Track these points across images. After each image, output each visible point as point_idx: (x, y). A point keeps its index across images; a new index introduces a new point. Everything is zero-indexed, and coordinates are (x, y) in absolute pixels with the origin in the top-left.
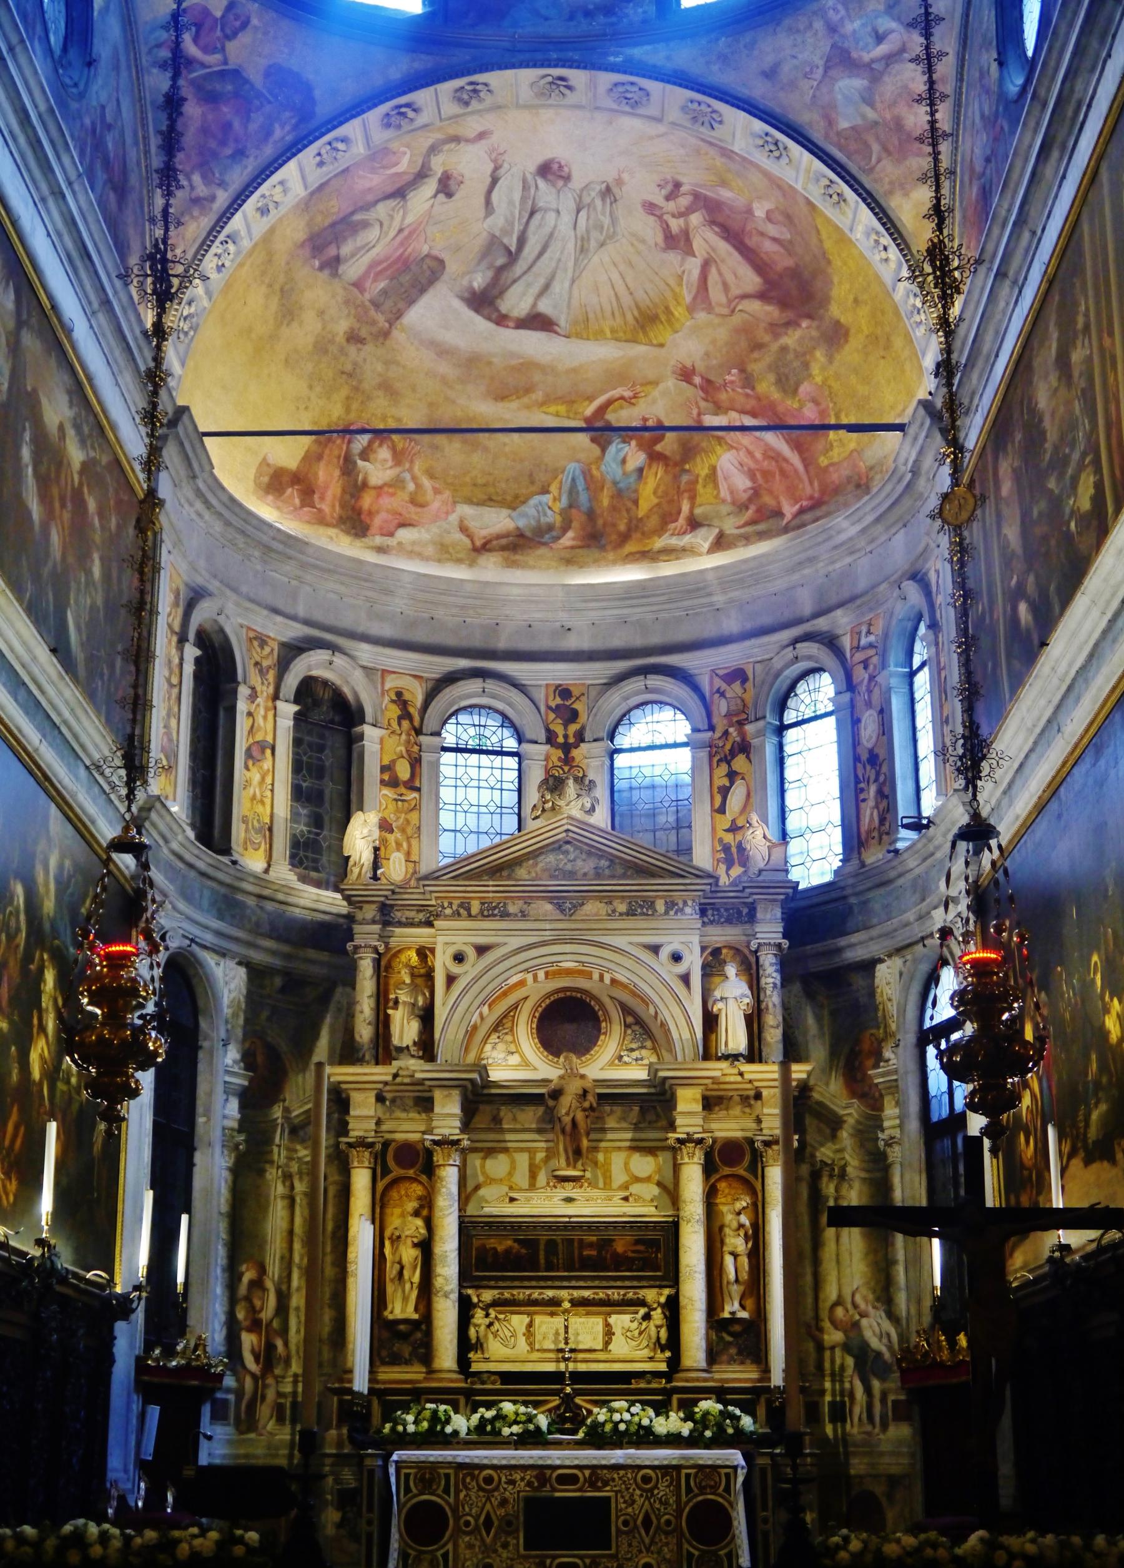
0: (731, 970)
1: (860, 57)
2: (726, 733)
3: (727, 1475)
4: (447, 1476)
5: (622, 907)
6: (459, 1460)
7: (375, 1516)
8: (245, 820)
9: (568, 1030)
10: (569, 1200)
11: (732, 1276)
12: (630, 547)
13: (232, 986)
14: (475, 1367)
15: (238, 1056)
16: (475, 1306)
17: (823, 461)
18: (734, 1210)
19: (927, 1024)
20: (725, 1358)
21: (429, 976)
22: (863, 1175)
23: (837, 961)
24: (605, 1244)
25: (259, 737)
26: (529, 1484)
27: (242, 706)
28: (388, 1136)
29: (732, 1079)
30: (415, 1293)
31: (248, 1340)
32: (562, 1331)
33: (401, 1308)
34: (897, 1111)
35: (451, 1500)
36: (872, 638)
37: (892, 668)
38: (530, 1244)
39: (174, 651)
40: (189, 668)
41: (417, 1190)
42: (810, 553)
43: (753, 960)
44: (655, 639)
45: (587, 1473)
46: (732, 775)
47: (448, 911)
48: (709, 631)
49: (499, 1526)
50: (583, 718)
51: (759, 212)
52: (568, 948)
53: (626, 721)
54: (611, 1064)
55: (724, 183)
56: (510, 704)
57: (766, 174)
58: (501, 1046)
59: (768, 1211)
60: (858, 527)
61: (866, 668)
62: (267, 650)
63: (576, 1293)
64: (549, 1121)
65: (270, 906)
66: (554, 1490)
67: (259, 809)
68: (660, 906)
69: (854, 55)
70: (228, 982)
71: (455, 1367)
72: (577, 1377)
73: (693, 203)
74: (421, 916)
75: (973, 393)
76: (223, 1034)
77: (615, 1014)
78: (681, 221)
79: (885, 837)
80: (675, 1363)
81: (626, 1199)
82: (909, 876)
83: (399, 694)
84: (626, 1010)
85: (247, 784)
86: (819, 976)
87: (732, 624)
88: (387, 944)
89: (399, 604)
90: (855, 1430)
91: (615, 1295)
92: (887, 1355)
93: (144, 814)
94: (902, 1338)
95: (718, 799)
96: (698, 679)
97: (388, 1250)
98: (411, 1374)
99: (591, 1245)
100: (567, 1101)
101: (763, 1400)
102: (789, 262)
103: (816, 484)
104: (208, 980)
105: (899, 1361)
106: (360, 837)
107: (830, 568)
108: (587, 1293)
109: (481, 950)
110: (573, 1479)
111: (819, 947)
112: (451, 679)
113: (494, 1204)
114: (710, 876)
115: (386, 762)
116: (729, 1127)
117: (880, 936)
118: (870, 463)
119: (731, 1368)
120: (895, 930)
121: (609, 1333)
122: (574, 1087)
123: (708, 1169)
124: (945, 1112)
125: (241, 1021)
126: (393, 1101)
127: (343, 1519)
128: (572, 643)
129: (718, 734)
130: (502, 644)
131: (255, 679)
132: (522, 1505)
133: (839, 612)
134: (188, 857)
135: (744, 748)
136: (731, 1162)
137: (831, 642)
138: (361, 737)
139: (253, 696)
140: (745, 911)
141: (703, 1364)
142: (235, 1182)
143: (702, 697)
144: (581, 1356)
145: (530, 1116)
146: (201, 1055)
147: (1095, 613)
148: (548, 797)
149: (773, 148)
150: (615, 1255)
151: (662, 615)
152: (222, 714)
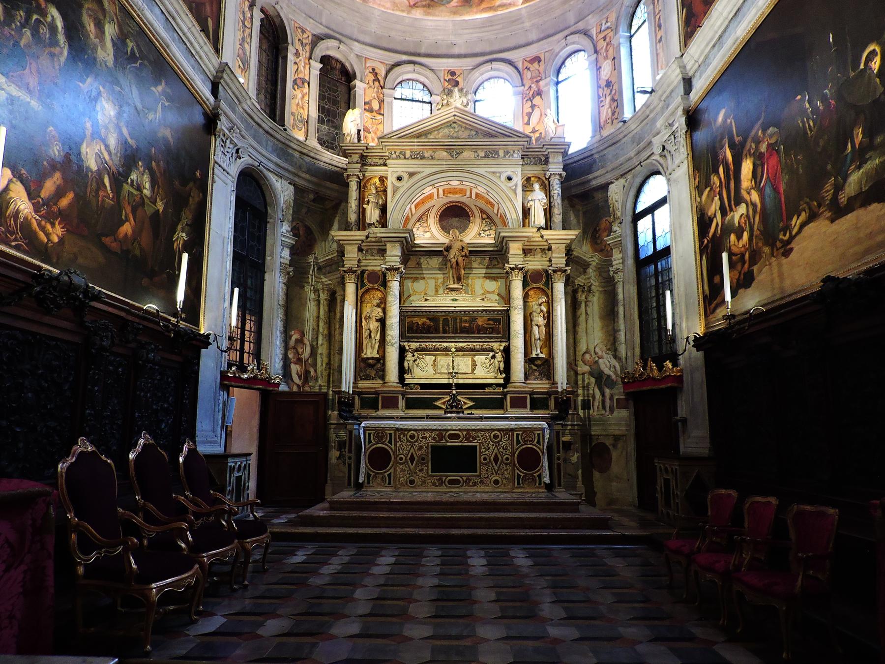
0: (537, 186)
2: (530, 87)
3: (539, 435)
4: (390, 434)
5: (482, 154)
6: (397, 426)
7: (353, 455)
8: (293, 114)
9: (455, 221)
10: (455, 300)
11: (537, 336)
12: (483, 6)
13: (286, 194)
14: (407, 381)
15: (289, 229)
16: (407, 351)
18: (537, 302)
20: (533, 377)
21: (385, 191)
22: (601, 289)
23: (587, 187)
24: (474, 320)
25: (301, 76)
26: (434, 439)
27: (291, 57)
28: (363, 268)
29: (537, 239)
30: (377, 345)
31: (295, 368)
32: (451, 364)
33: (371, 352)
34: (621, 256)
35: (393, 447)
36: (609, 24)
37: (621, 33)
38: (435, 320)
39: (247, 9)
40: (257, 23)
41: (379, 294)
43: (547, 183)
44: (496, 47)
45: (464, 433)
46: (533, 107)
47: (394, 156)
48: (522, 41)
49: (418, 461)
50: (461, 85)
52: (455, 174)
53: (481, 87)
54: (475, 237)
56: (427, 78)
58: (421, 229)
59: (555, 305)
62: (305, 35)
63: (458, 345)
64: (445, 264)
65: (307, 159)
66: (447, 442)
67: (301, 111)
68: (501, 153)
70: (283, 192)
71: (397, 380)
72: (459, 386)
74: (381, 161)
76: (280, 216)
77: (477, 213)
79: (615, 121)
80: (507, 380)
81: (483, 299)
82: (630, 135)
83: (373, 70)
84: (482, 212)
85: (294, 97)
86: (577, 196)
87: (533, 36)
88: (364, 175)
89: (373, 27)
90: (595, 413)
91: (478, 346)
92: (614, 377)
93: (220, 74)
94: (622, 367)
95: (526, 119)
96: (516, 64)
97: (364, 324)
98: (376, 384)
99: (466, 321)
100: (453, 253)
101: (552, 397)
104: (271, 187)
105: (623, 379)
106: (352, 121)
108: (463, 345)
109: (411, 175)
110: (458, 436)
111: (578, 181)
112: (398, 64)
113: (417, 302)
114: (528, 137)
115: (367, 100)
116: (535, 264)
117: (612, 170)
119: (535, 382)
120: (622, 164)
121: (474, 365)
122: (457, 246)
123: (525, 284)
124: (650, 251)
125: (291, 212)
126: (367, 251)
127: (340, 454)
128: (456, 51)
129: (527, 87)
130: (423, 50)
131: (298, 46)
132: (430, 450)
133: (590, 16)
134: (256, 118)
135: (539, 93)
136: (536, 282)
137: (586, 33)
138: (355, 87)
139: (297, 54)
140: (543, 159)
141: (523, 380)
142: (287, 290)
143: (519, 72)
144: (460, 376)
145: (435, 262)
146: (268, 225)
148: (445, 97)
150: (478, 326)
151: (499, 36)
152: (280, 60)
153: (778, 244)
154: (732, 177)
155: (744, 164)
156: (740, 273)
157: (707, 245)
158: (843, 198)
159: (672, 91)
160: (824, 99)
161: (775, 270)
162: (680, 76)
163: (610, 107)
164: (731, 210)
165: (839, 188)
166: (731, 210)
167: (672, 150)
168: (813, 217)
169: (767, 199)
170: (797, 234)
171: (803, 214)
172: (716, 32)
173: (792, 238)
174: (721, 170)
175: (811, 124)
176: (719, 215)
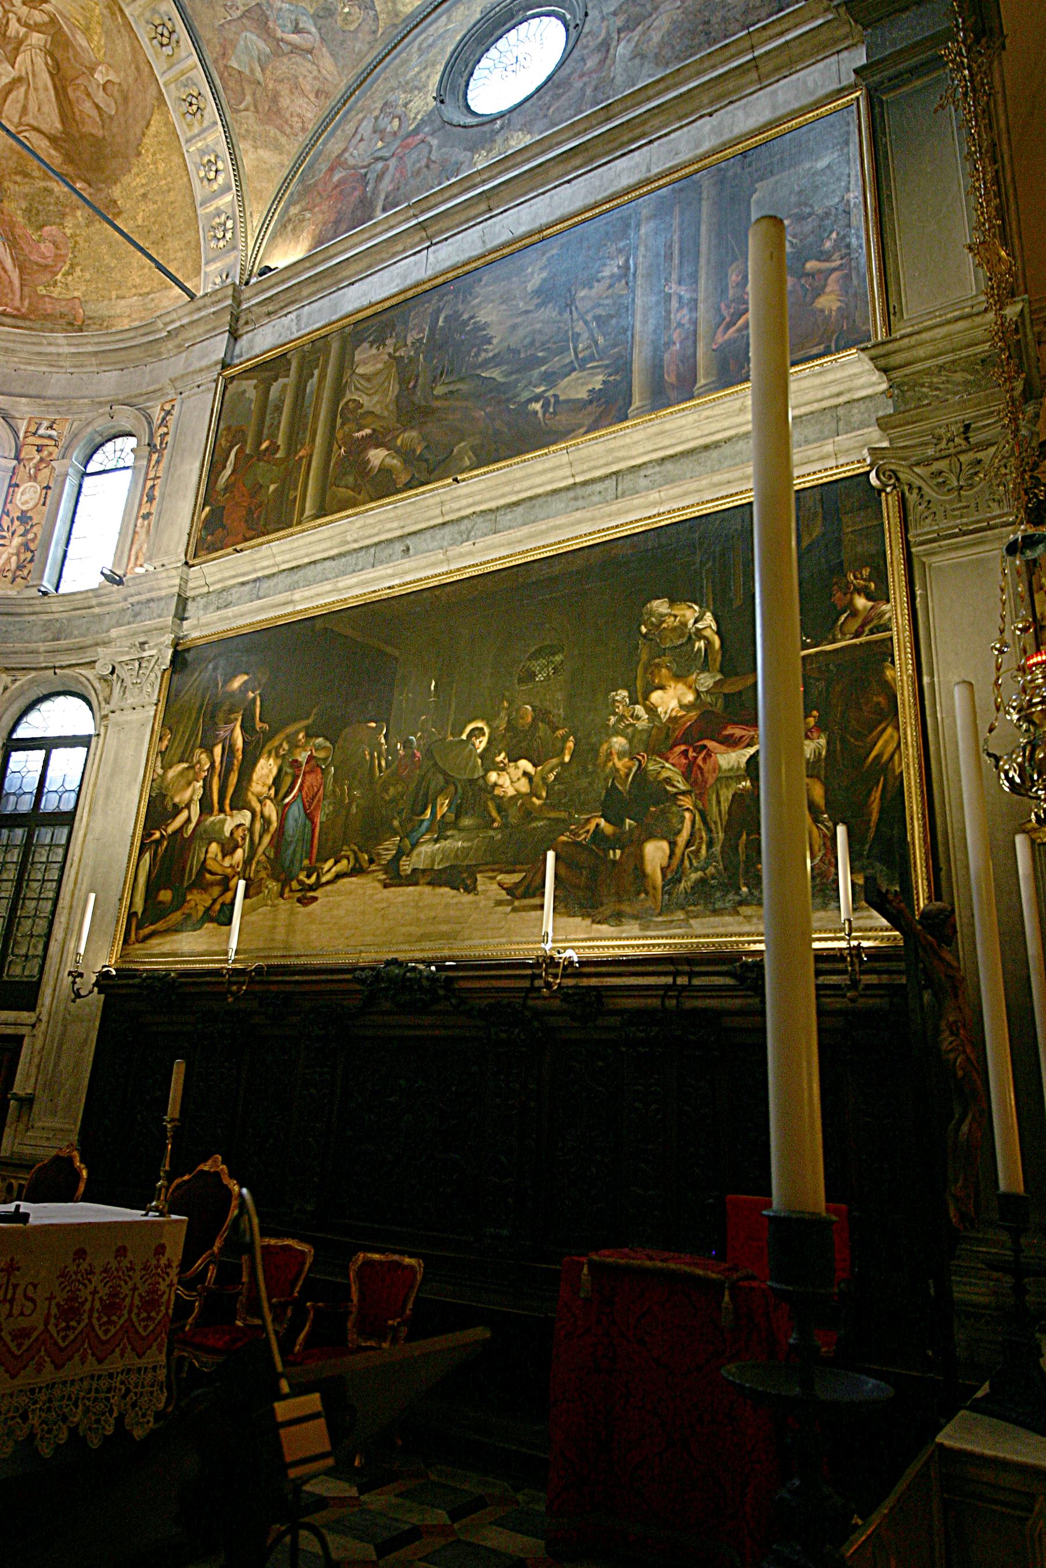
1: (275, 30)
17: (42, 290)
19: (15, 736)
42: (11, 345)
51: (99, 77)
55: (87, 31)
57: (136, 48)
60: (73, 350)
61: (38, 451)
69: (271, 24)
73: (45, 24)
75: (293, 302)
78: (23, 30)
82: (46, 617)
102: (99, 133)
103: (26, 303)
107: (22, 367)
118: (89, 314)
120: (15, 653)
147: (567, 471)
149: (166, 33)
153: (295, 885)
154: (236, 768)
155: (262, 762)
156: (214, 901)
157: (158, 842)
158: (406, 866)
159: (152, 600)
160: (407, 744)
161: (283, 916)
162: (176, 590)
163: (18, 554)
164: (222, 810)
165: (400, 853)
166: (222, 810)
167: (128, 682)
168: (357, 871)
169: (290, 822)
170: (328, 883)
171: (345, 862)
172: (255, 571)
173: (318, 885)
174: (218, 750)
175: (383, 763)
176: (195, 809)
